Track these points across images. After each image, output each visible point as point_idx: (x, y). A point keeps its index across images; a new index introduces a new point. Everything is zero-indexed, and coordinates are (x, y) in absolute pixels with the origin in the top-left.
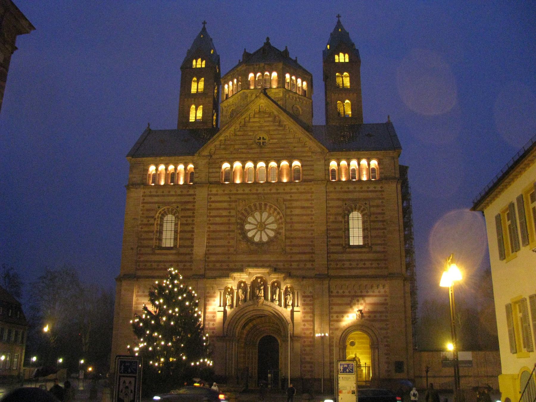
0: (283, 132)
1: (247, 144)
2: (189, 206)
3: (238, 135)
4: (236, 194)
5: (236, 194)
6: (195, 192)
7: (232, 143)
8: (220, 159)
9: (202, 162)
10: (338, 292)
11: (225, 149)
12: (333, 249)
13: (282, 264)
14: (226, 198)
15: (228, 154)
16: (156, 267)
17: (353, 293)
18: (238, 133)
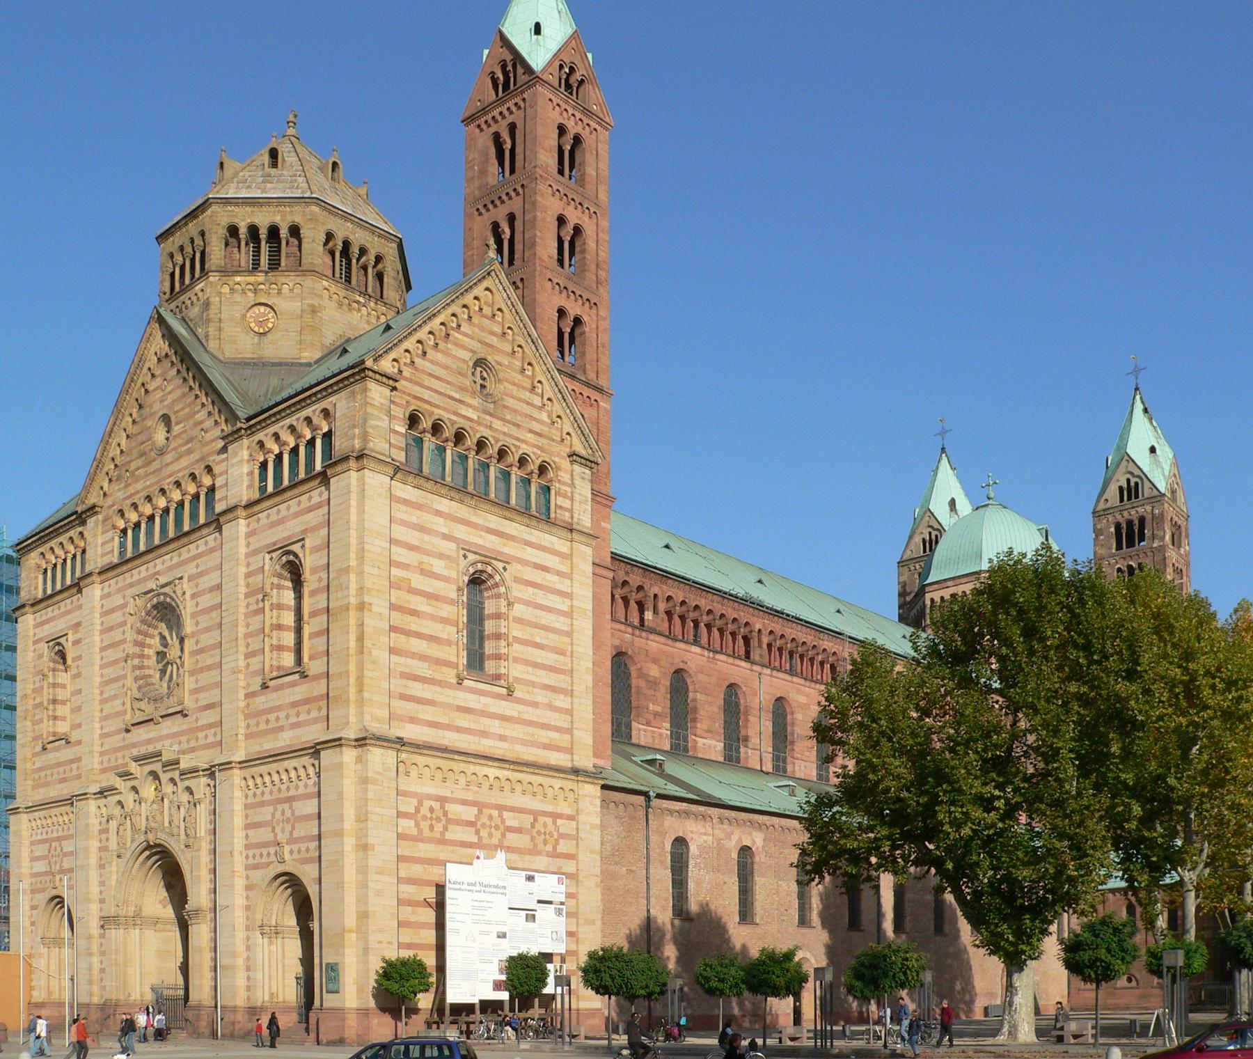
4: (131, 585)
5: (131, 585)
8: (112, 506)
11: (119, 478)
17: (276, 795)
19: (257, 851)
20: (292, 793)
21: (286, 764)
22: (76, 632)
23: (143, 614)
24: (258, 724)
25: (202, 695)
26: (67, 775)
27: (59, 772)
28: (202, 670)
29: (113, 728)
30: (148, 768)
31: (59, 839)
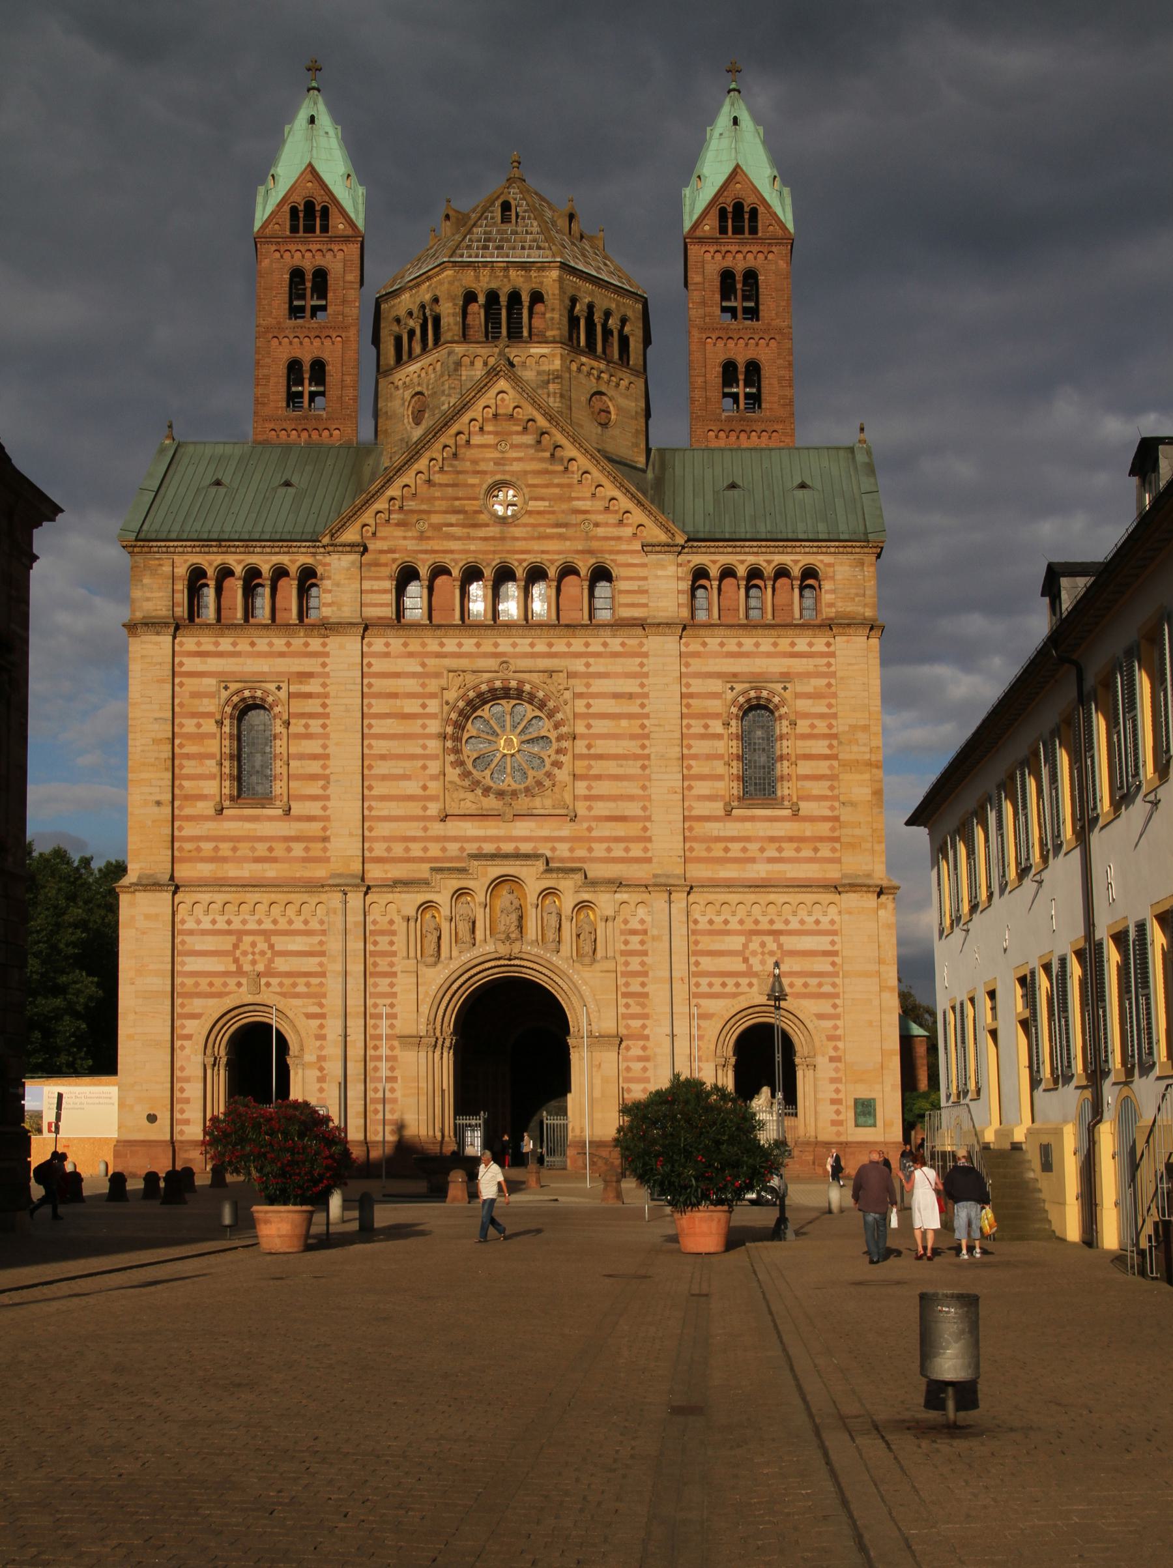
0: (564, 480)
1: (465, 512)
2: (313, 687)
3: (441, 485)
4: (439, 655)
5: (439, 655)
6: (324, 645)
7: (424, 507)
8: (391, 551)
9: (339, 559)
10: (711, 922)
12: (701, 809)
13: (566, 846)
14: (413, 666)
15: (413, 538)
16: (229, 853)
18: (437, 478)
19: (717, 981)
20: (779, 926)
21: (772, 897)
22: (301, 683)
23: (471, 694)
24: (709, 849)
25: (600, 804)
26: (273, 855)
27: (261, 849)
28: (599, 777)
29: (400, 812)
30: (495, 871)
31: (266, 934)
